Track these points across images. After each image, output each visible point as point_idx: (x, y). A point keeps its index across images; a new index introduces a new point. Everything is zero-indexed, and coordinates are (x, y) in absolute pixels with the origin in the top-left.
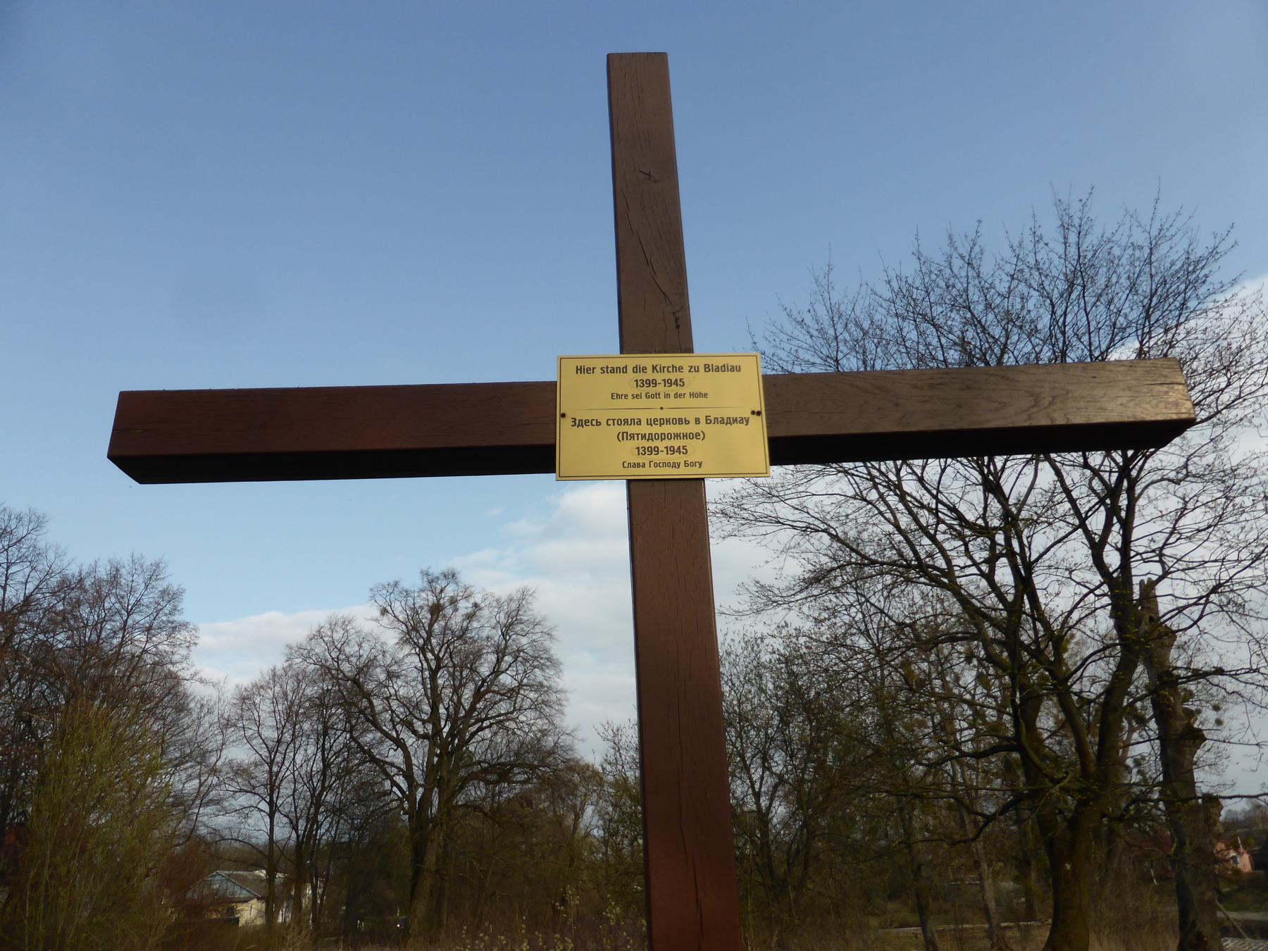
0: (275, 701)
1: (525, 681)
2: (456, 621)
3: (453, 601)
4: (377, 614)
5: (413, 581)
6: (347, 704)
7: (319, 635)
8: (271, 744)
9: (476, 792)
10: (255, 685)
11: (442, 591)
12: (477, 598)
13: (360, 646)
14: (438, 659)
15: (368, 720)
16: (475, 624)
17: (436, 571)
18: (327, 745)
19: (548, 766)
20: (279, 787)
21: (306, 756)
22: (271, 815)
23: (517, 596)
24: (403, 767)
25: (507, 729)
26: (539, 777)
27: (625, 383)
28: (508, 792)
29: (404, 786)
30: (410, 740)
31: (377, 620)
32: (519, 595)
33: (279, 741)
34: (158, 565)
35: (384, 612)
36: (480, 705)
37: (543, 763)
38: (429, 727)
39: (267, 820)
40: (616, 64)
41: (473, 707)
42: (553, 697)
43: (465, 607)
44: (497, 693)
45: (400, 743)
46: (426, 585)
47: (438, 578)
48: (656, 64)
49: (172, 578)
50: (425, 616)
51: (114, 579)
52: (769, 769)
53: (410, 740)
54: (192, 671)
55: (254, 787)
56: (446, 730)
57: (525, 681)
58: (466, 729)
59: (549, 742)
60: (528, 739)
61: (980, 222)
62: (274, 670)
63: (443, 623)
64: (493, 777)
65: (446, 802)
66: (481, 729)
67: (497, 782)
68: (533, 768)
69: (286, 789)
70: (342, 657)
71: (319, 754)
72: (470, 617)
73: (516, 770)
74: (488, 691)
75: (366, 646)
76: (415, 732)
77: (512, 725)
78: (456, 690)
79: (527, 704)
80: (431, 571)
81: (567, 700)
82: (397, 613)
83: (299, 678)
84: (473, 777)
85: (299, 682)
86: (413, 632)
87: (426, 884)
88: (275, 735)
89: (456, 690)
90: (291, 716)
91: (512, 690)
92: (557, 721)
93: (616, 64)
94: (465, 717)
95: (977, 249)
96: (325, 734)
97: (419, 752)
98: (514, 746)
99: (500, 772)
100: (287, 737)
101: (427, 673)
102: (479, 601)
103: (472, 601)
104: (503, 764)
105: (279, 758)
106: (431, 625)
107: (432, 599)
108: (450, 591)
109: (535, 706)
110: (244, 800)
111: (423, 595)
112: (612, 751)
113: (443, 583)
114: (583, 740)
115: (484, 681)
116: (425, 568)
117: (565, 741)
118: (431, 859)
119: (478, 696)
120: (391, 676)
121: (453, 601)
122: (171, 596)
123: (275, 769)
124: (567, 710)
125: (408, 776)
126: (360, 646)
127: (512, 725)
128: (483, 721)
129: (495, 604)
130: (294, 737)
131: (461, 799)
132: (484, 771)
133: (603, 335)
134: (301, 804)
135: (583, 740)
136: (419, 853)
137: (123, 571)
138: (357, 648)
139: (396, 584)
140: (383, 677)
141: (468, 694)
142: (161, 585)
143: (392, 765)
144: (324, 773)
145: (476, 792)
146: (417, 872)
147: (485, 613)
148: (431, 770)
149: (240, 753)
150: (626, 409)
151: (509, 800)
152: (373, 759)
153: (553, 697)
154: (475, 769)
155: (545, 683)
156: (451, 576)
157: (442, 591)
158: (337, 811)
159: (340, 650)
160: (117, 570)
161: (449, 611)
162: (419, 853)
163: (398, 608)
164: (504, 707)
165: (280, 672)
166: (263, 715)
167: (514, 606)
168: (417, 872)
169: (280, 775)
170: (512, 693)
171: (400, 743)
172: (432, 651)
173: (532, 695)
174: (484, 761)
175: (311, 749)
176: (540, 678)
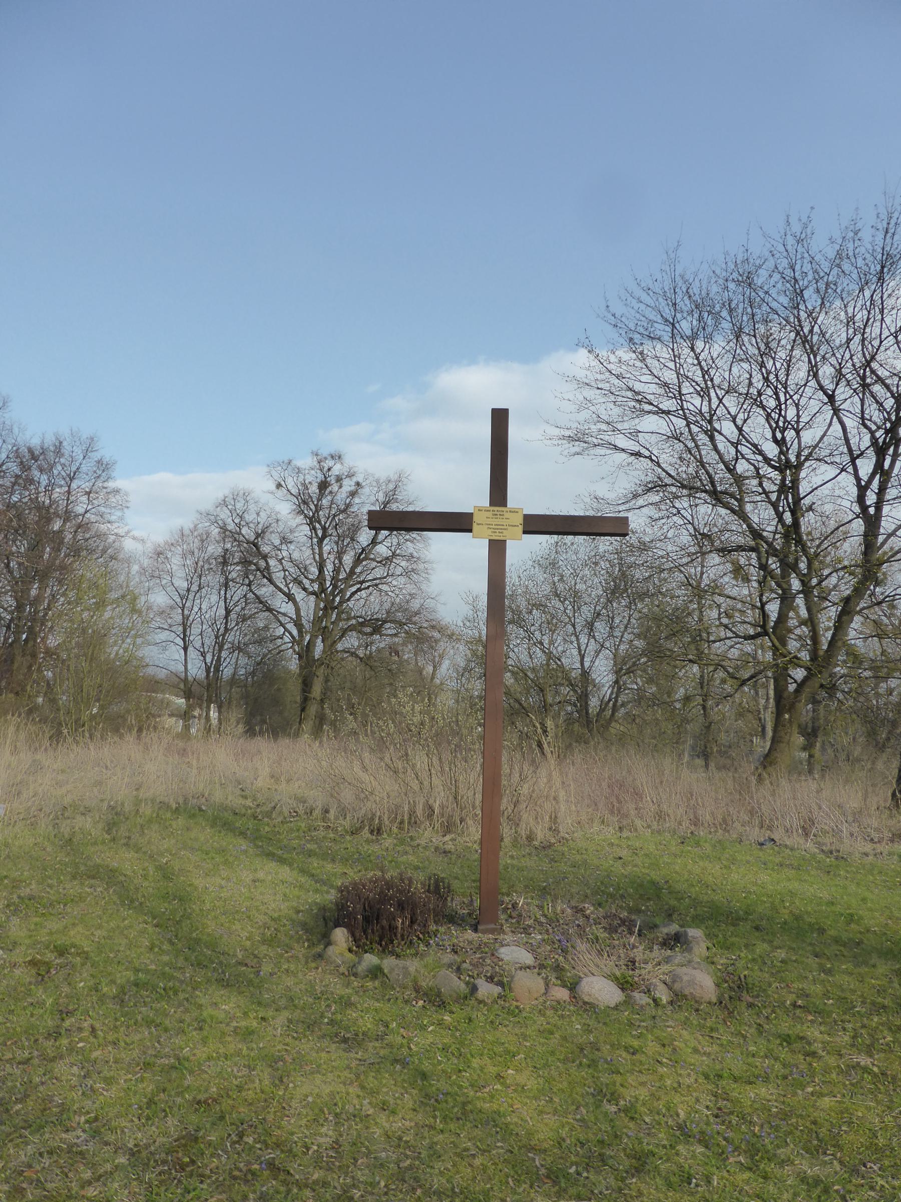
0: (184, 556)
1: (398, 551)
2: (341, 496)
3: (339, 479)
4: (273, 487)
5: (306, 462)
6: (245, 562)
7: (224, 503)
8: (182, 592)
9: (352, 641)
10: (166, 543)
11: (329, 470)
12: (359, 478)
13: (258, 514)
14: (324, 529)
15: (264, 577)
16: (357, 500)
17: (325, 452)
18: (228, 596)
19: (415, 623)
20: (190, 627)
21: (211, 604)
22: (185, 649)
23: (394, 477)
24: (294, 617)
25: (381, 590)
26: (406, 632)
27: (490, 514)
28: (380, 643)
29: (295, 632)
30: (299, 595)
31: (272, 493)
32: (396, 477)
33: (188, 590)
34: (92, 439)
35: (279, 486)
36: (358, 570)
37: (410, 621)
38: (316, 586)
39: (182, 652)
40: (494, 411)
41: (352, 572)
42: (421, 566)
43: (348, 485)
44: (373, 560)
45: (290, 597)
46: (315, 463)
47: (326, 458)
48: (506, 411)
49: (106, 451)
50: (314, 489)
51: (58, 450)
52: (594, 637)
53: (299, 595)
54: (126, 529)
55: (171, 626)
56: (329, 589)
57: (398, 551)
58: (346, 588)
59: (415, 605)
60: (398, 600)
61: (812, 208)
62: (182, 530)
63: (329, 498)
64: (368, 630)
65: (330, 647)
66: (359, 590)
67: (371, 634)
68: (401, 624)
69: (195, 630)
70: (243, 523)
71: (222, 604)
72: (353, 494)
73: (387, 625)
74: (366, 559)
75: (262, 514)
76: (305, 589)
77: (384, 587)
78: (340, 555)
79: (399, 571)
80: (320, 452)
81: (432, 569)
82: (290, 487)
83: (204, 539)
84: (351, 628)
85: (202, 541)
86: (303, 501)
87: (313, 709)
88: (185, 585)
89: (340, 555)
90: (198, 572)
91: (387, 558)
92: (423, 587)
93: (494, 411)
94: (346, 579)
95: (809, 231)
96: (226, 585)
97: (308, 606)
98: (387, 606)
99: (375, 626)
100: (195, 588)
101: (315, 540)
102: (361, 481)
103: (355, 479)
104: (377, 620)
105: (188, 604)
106: (319, 500)
107: (320, 477)
108: (337, 469)
109: (407, 573)
110: (164, 636)
111: (313, 472)
112: (471, 612)
113: (330, 463)
114: (444, 604)
115: (363, 550)
116: (315, 449)
117: (430, 603)
118: (317, 690)
119: (358, 561)
120: (285, 540)
121: (339, 479)
122: (104, 468)
123: (186, 612)
124: (433, 578)
125: (298, 624)
126: (258, 514)
127: (384, 587)
128: (362, 583)
129: (375, 484)
130: (200, 588)
131: (340, 646)
132: (362, 624)
133: (486, 502)
134: (207, 642)
135: (444, 604)
136: (306, 685)
137: (65, 444)
138: (255, 516)
139: (290, 462)
140: (277, 542)
141: (348, 559)
142: (96, 456)
143: (284, 615)
144: (226, 617)
145: (352, 641)
146: (305, 700)
147: (366, 491)
148: (317, 620)
149: (159, 599)
150: (489, 521)
151: (379, 650)
152: (269, 610)
153: (421, 566)
154: (354, 622)
155: (415, 554)
156: (337, 457)
157: (329, 470)
158: (239, 648)
159: (241, 517)
160: (61, 443)
161: (335, 488)
162: (306, 685)
163: (290, 483)
164: (379, 572)
165: (186, 532)
166: (175, 568)
167: (391, 486)
168: (305, 700)
169: (191, 619)
170: (386, 561)
171: (290, 597)
172: (319, 523)
173: (403, 564)
174: (360, 617)
175: (214, 598)
176: (411, 550)
